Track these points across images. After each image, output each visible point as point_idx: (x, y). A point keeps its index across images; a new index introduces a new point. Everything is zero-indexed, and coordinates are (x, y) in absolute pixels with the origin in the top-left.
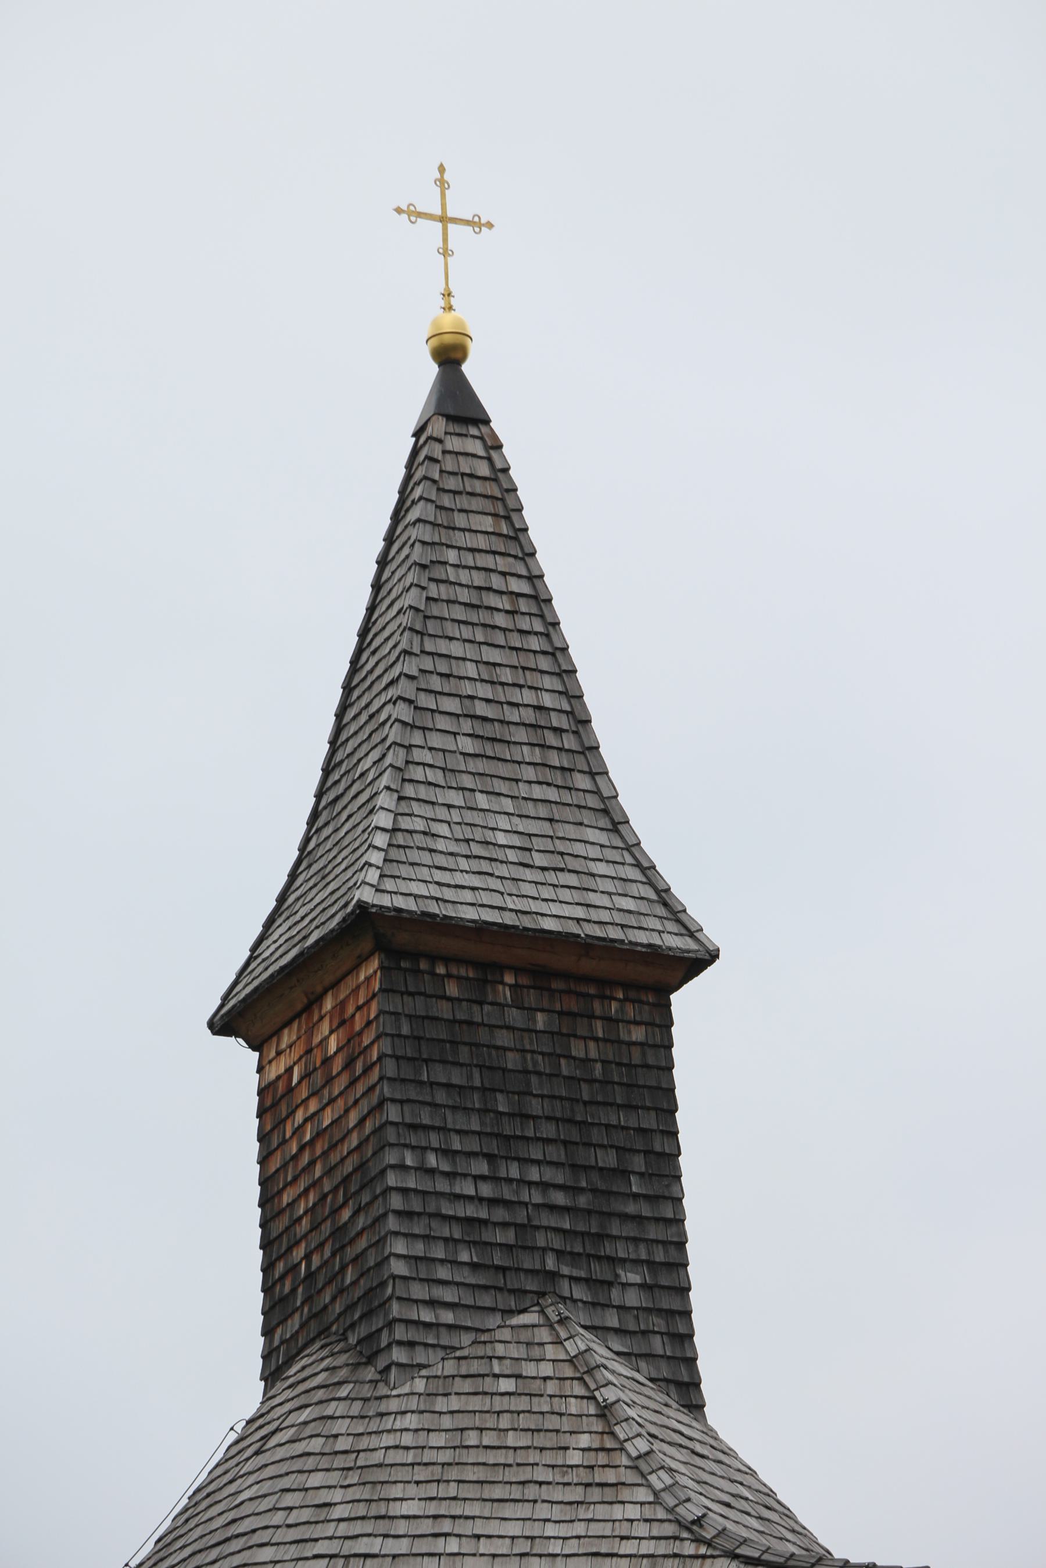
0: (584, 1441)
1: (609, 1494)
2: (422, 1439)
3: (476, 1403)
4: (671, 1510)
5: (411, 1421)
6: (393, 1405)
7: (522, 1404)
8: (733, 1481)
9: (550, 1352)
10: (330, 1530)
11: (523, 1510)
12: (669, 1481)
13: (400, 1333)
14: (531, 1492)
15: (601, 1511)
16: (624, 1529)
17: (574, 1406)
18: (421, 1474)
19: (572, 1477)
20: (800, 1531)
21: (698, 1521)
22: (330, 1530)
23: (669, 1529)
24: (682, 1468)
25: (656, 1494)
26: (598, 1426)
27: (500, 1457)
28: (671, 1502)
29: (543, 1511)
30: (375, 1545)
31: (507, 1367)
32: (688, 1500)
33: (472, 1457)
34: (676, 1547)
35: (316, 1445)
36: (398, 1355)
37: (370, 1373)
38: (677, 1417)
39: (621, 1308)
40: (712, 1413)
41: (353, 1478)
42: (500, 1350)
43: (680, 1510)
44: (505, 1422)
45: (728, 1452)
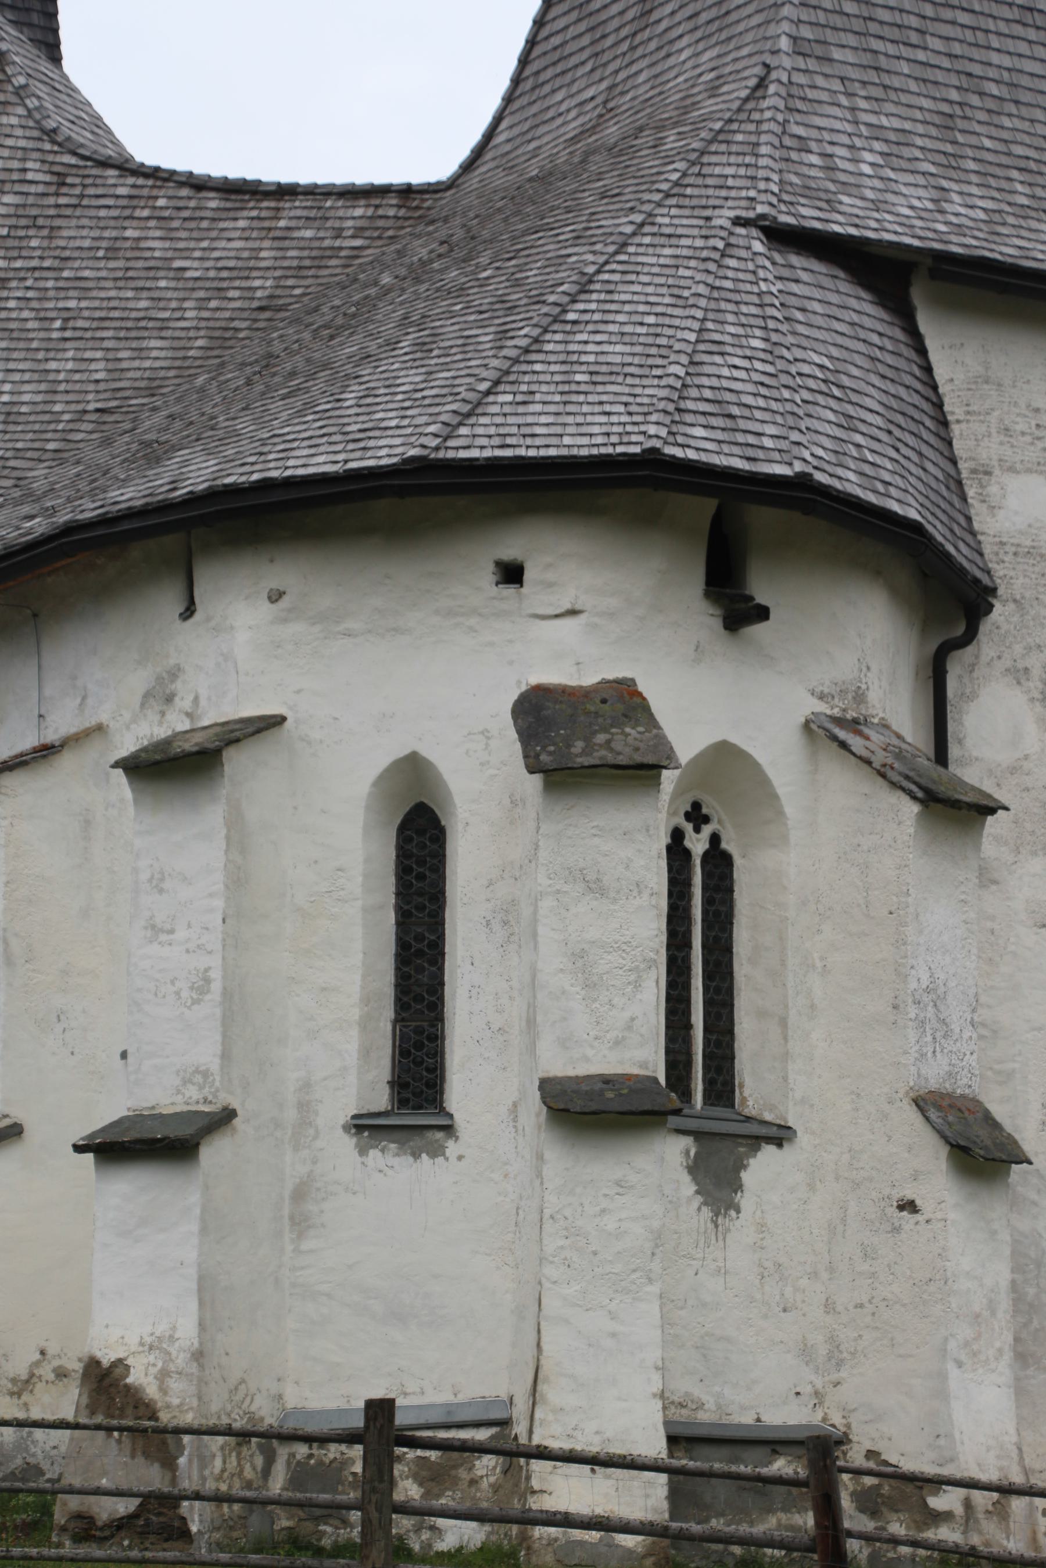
4: (37, 122)
8: (76, 108)
12: (36, 103)
23: (36, 133)
24: (46, 97)
25: (29, 110)
28: (38, 116)
32: (49, 117)
34: (39, 145)
38: (45, 66)
40: (65, 63)
43: (44, 123)
45: (75, 90)
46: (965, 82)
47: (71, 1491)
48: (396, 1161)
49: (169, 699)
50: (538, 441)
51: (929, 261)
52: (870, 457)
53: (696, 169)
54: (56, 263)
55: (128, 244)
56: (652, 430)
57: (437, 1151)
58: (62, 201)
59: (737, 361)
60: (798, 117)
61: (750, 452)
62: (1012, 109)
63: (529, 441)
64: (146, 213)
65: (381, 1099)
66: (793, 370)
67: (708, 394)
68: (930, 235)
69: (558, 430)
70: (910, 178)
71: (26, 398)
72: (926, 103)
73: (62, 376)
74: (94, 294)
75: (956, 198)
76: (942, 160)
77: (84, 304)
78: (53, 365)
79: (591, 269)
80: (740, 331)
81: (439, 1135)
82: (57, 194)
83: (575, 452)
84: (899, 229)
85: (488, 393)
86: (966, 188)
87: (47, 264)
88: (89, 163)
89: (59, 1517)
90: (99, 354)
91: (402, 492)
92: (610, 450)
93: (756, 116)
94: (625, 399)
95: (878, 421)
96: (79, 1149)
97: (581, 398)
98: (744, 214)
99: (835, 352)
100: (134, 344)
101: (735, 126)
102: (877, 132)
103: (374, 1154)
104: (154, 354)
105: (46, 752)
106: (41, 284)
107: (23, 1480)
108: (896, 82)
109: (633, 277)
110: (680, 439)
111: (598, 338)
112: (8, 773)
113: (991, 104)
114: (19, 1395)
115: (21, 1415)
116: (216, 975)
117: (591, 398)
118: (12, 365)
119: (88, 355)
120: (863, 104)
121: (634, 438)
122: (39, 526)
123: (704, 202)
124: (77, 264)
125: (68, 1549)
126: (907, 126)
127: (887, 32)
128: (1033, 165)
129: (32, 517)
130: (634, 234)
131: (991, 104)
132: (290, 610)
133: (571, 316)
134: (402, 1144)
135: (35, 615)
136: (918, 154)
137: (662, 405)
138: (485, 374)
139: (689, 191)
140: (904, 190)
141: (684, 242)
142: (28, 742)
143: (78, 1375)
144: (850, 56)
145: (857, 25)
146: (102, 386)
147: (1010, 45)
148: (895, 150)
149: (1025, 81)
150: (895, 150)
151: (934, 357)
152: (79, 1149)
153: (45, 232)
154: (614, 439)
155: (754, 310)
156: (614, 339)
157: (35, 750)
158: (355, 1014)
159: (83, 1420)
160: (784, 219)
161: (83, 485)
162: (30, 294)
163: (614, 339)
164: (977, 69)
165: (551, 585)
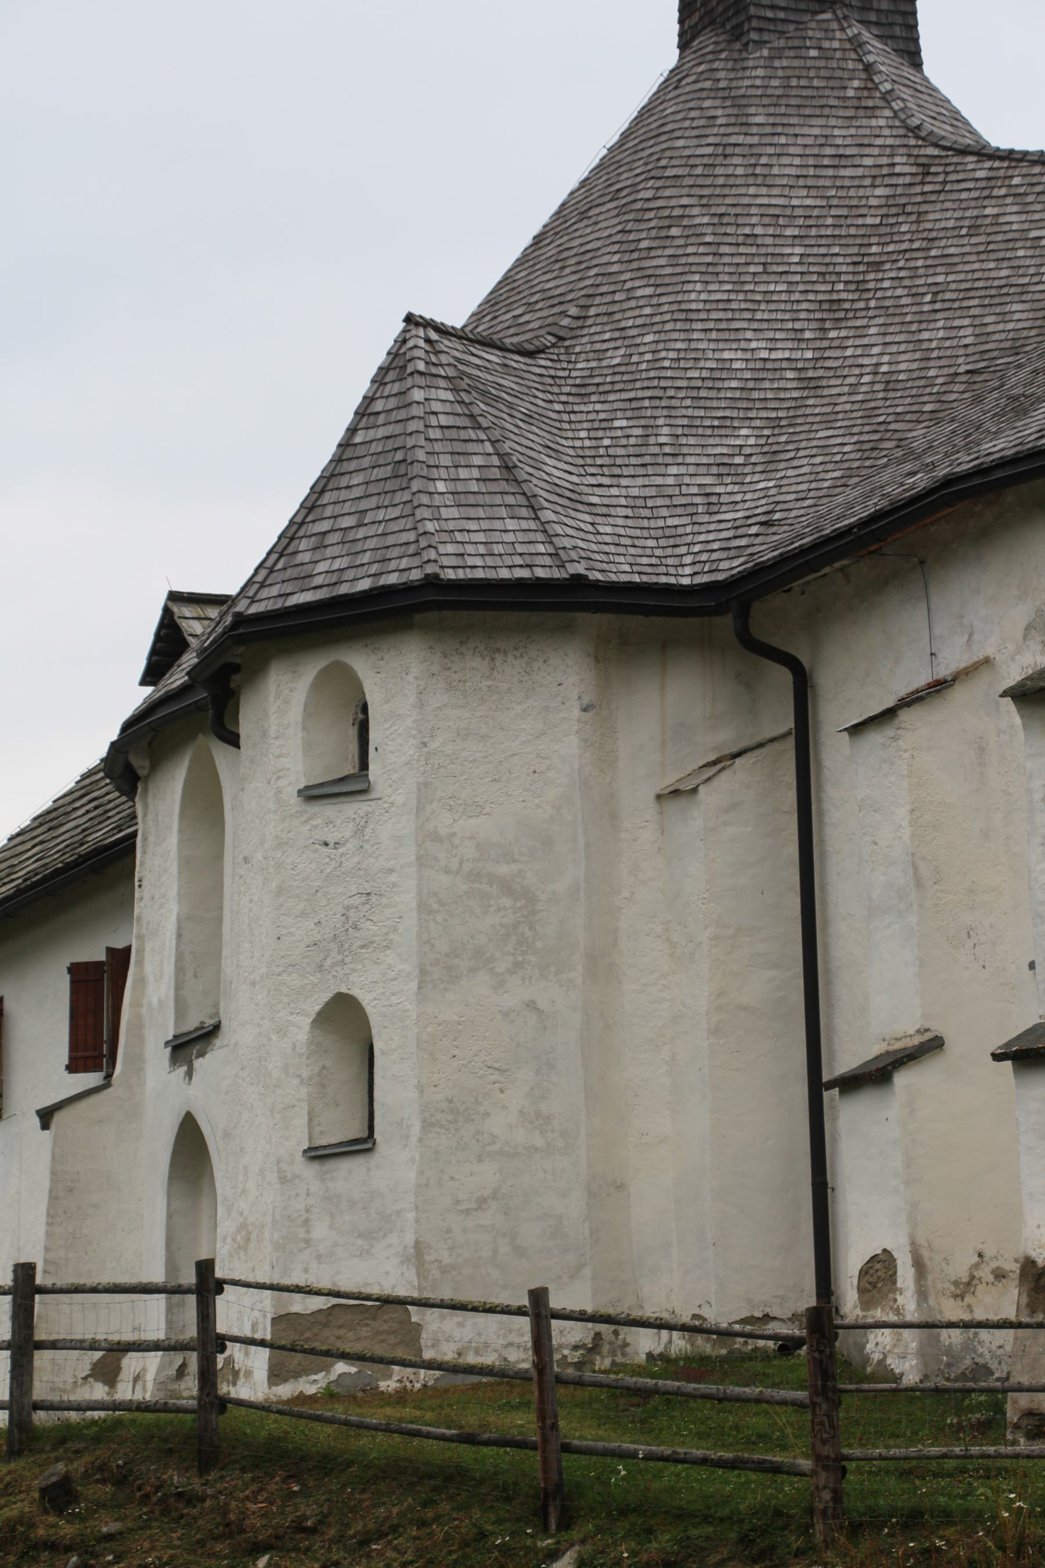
0: (856, 83)
1: (869, 113)
2: (766, 82)
3: (796, 63)
4: (903, 121)
5: (760, 72)
6: (750, 63)
7: (822, 63)
8: (937, 105)
9: (838, 35)
10: (715, 131)
11: (821, 121)
12: (902, 105)
13: (755, 23)
14: (826, 111)
15: (864, 122)
16: (877, 132)
17: (851, 65)
18: (765, 101)
19: (849, 103)
20: (973, 132)
21: (918, 127)
22: (715, 131)
23: (902, 132)
24: (910, 99)
25: (895, 112)
26: (863, 76)
27: (809, 92)
28: (903, 116)
29: (833, 122)
30: (740, 139)
31: (814, 43)
32: (913, 115)
33: (793, 92)
34: (905, 141)
35: (708, 84)
36: (754, 36)
37: (738, 46)
38: (907, 72)
39: (878, 11)
40: (926, 68)
41: (728, 103)
42: (810, 33)
43: (908, 121)
44: (812, 73)
45: (935, 90)
47: (1020, 1389)
54: (924, 244)
58: (927, 188)
71: (903, 367)
73: (934, 345)
74: (960, 268)
77: (950, 278)
78: (925, 335)
82: (923, 183)
87: (916, 245)
88: (950, 153)
89: (1012, 1415)
96: (997, 1057)
105: (939, 687)
106: (912, 264)
107: (974, 1380)
112: (906, 709)
114: (962, 1297)
115: (966, 1317)
118: (888, 339)
119: (957, 323)
122: (921, 481)
124: (943, 243)
125: (1023, 1446)
129: (914, 473)
135: (922, 562)
142: (922, 679)
143: (1016, 1276)
152: (997, 1057)
153: (913, 218)
157: (930, 686)
159: (1025, 1319)
161: (958, 441)
162: (902, 274)
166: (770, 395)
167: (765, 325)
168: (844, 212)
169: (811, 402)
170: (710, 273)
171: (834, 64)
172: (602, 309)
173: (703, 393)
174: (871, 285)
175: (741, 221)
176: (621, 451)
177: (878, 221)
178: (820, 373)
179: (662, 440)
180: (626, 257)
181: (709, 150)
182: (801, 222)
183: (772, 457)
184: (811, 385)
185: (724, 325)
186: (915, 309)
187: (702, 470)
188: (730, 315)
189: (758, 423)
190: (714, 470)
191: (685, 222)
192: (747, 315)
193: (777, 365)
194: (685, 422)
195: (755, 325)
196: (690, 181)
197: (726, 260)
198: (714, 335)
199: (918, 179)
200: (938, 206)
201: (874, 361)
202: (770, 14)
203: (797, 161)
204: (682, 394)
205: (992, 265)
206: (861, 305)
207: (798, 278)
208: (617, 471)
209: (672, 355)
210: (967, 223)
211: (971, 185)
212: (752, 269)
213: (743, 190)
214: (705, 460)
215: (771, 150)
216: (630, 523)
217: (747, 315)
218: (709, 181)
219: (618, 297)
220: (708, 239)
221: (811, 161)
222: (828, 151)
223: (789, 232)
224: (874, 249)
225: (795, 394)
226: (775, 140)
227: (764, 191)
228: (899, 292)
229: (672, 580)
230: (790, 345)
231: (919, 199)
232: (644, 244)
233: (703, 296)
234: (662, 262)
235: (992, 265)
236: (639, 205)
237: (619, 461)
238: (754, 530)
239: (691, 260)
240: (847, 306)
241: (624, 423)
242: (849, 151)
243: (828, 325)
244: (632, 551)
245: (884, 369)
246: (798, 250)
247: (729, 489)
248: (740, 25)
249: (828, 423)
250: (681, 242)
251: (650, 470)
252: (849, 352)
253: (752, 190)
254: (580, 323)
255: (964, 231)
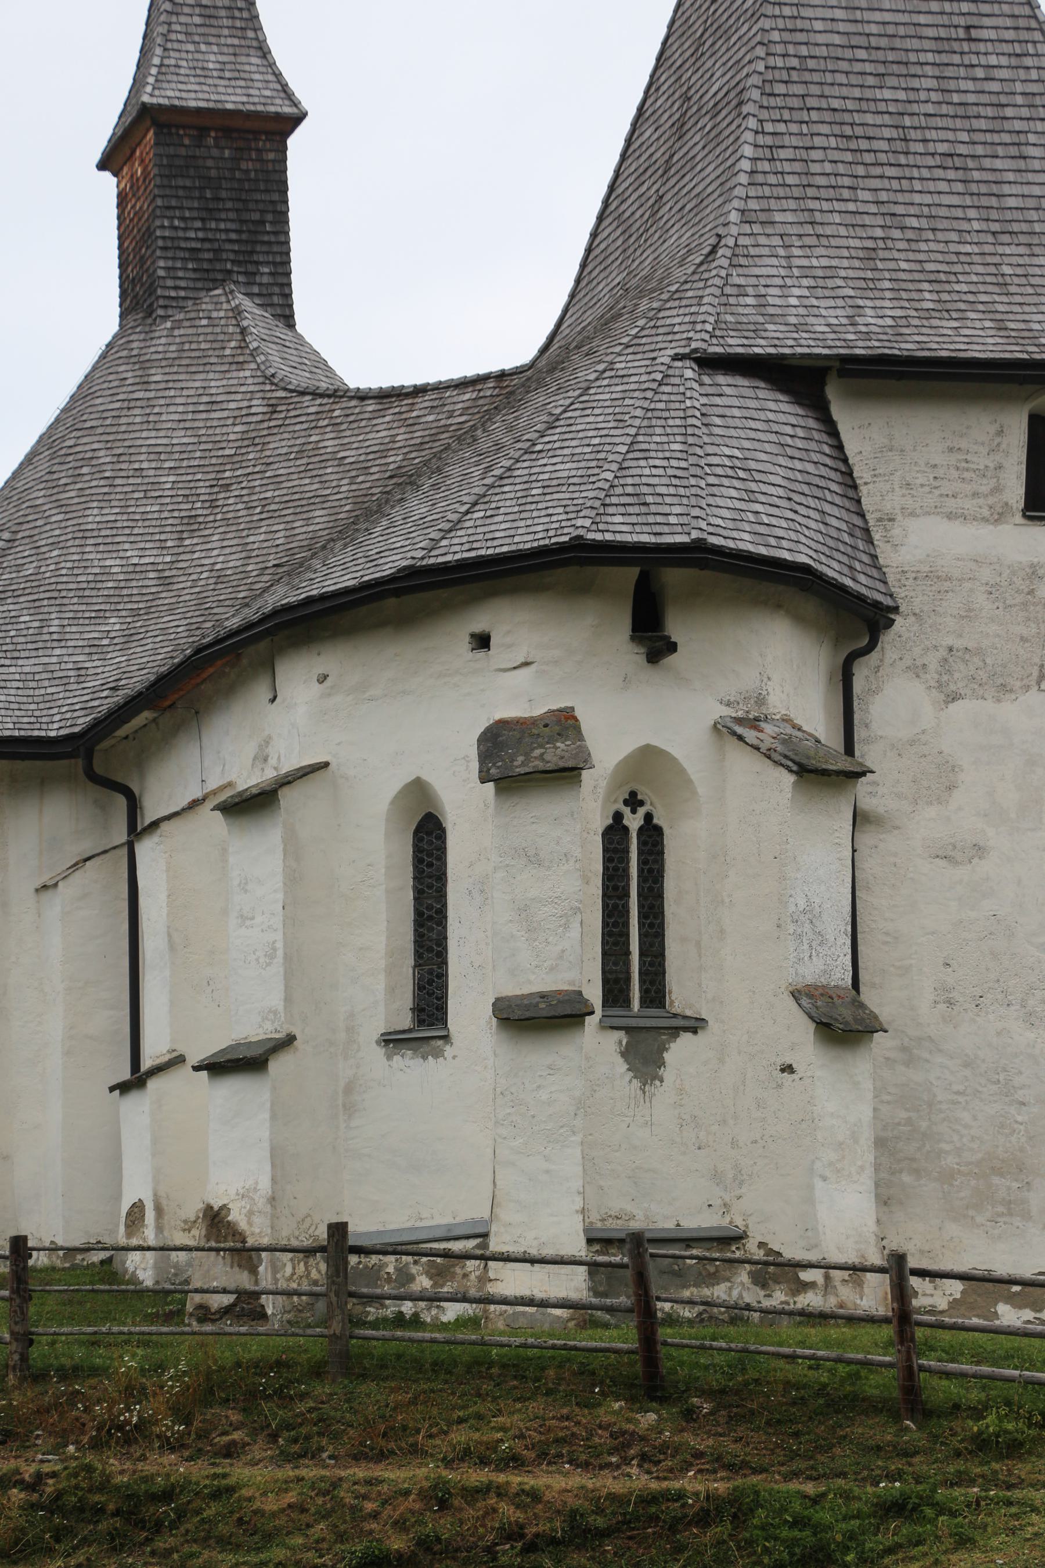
0: (233, 344)
1: (239, 367)
2: (166, 348)
3: (190, 331)
5: (163, 341)
6: (157, 334)
7: (209, 330)
9: (225, 306)
10: (124, 389)
13: (161, 302)
14: (208, 368)
15: (235, 374)
16: (242, 381)
17: (231, 329)
18: (164, 363)
19: (226, 360)
21: (273, 376)
22: (124, 389)
26: (239, 337)
29: (211, 376)
31: (206, 314)
33: (185, 354)
35: (124, 353)
37: (149, 321)
39: (260, 284)
41: (137, 367)
42: (204, 307)
44: (201, 338)
46: (888, 221)
48: (411, 1063)
49: (266, 760)
50: (496, 543)
51: (837, 364)
52: (766, 519)
53: (652, 324)
54: (263, 468)
55: (310, 447)
56: (579, 522)
57: (438, 1054)
59: (657, 463)
60: (740, 271)
61: (657, 529)
62: (930, 235)
63: (489, 544)
64: (326, 422)
65: (405, 1020)
66: (702, 462)
67: (629, 490)
68: (838, 343)
69: (512, 532)
70: (831, 303)
72: (852, 243)
73: (255, 546)
74: (284, 485)
75: (869, 312)
76: (863, 284)
77: (277, 493)
78: (251, 539)
79: (558, 411)
80: (665, 439)
81: (440, 1043)
83: (521, 546)
84: (812, 343)
85: (467, 512)
86: (879, 303)
87: (257, 469)
90: (281, 527)
91: (397, 593)
92: (547, 542)
93: (706, 276)
94: (564, 503)
95: (781, 492)
97: (533, 506)
98: (681, 351)
99: (747, 444)
100: (305, 516)
101: (687, 286)
102: (807, 272)
103: (397, 1058)
104: (317, 520)
106: (252, 484)
108: (829, 230)
109: (589, 412)
110: (601, 527)
111: (555, 460)
113: (910, 234)
116: (280, 945)
117: (540, 506)
119: (275, 528)
120: (797, 252)
121: (566, 531)
123: (653, 347)
124: (275, 466)
126: (834, 263)
127: (824, 193)
128: (943, 277)
130: (597, 379)
131: (910, 234)
132: (332, 687)
133: (538, 448)
134: (415, 1050)
136: (840, 282)
137: (589, 504)
138: (465, 499)
139: (644, 341)
140: (824, 312)
141: (633, 379)
144: (790, 217)
145: (797, 192)
146: (281, 548)
147: (931, 186)
148: (821, 282)
149: (943, 212)
150: (821, 282)
151: (844, 437)
153: (259, 448)
154: (551, 533)
155: (678, 422)
156: (566, 459)
158: (382, 964)
160: (712, 350)
162: (244, 492)
163: (566, 459)
164: (900, 210)
165: (510, 646)
166: (135, 591)
167: (139, 538)
168: (210, 446)
169: (163, 595)
170: (105, 500)
171: (218, 330)
172: (27, 533)
173: (87, 593)
174: (220, 503)
175: (133, 458)
176: (22, 640)
177: (232, 452)
178: (174, 572)
179: (52, 629)
180: (50, 492)
181: (118, 405)
182: (177, 456)
183: (129, 638)
184: (165, 582)
185: (109, 540)
186: (248, 519)
187: (78, 651)
188: (114, 532)
189: (124, 613)
190: (87, 650)
191: (94, 462)
192: (127, 531)
193: (144, 568)
194: (71, 615)
195: (132, 539)
196: (100, 430)
197: (119, 489)
198: (101, 548)
199: (267, 417)
200: (279, 437)
201: (212, 561)
202: (173, 294)
203: (181, 409)
204: (71, 594)
205: (307, 481)
206: (211, 518)
207: (168, 500)
208: (16, 654)
209: (69, 565)
210: (296, 449)
211: (303, 419)
212: (136, 495)
213: (137, 435)
214: (81, 643)
215: (162, 402)
216: (20, 692)
217: (127, 531)
218: (114, 429)
219: (39, 523)
220: (107, 474)
221: (191, 408)
222: (205, 399)
223: (167, 465)
224: (227, 474)
225: (154, 590)
226: (167, 393)
227: (153, 434)
228: (240, 506)
229: (43, 734)
230: (155, 552)
231: (265, 432)
232: (63, 481)
233: (98, 519)
234: (72, 494)
235: (307, 481)
236: (63, 452)
237: (19, 647)
238: (105, 694)
239: (93, 491)
240: (201, 519)
241: (27, 618)
242: (219, 398)
243: (185, 535)
244: (17, 713)
245: (218, 567)
246: (172, 479)
247: (95, 664)
248: (151, 304)
249: (171, 611)
250: (88, 478)
251: (41, 653)
252: (196, 555)
253: (145, 434)
254: (10, 545)
255: (292, 456)
